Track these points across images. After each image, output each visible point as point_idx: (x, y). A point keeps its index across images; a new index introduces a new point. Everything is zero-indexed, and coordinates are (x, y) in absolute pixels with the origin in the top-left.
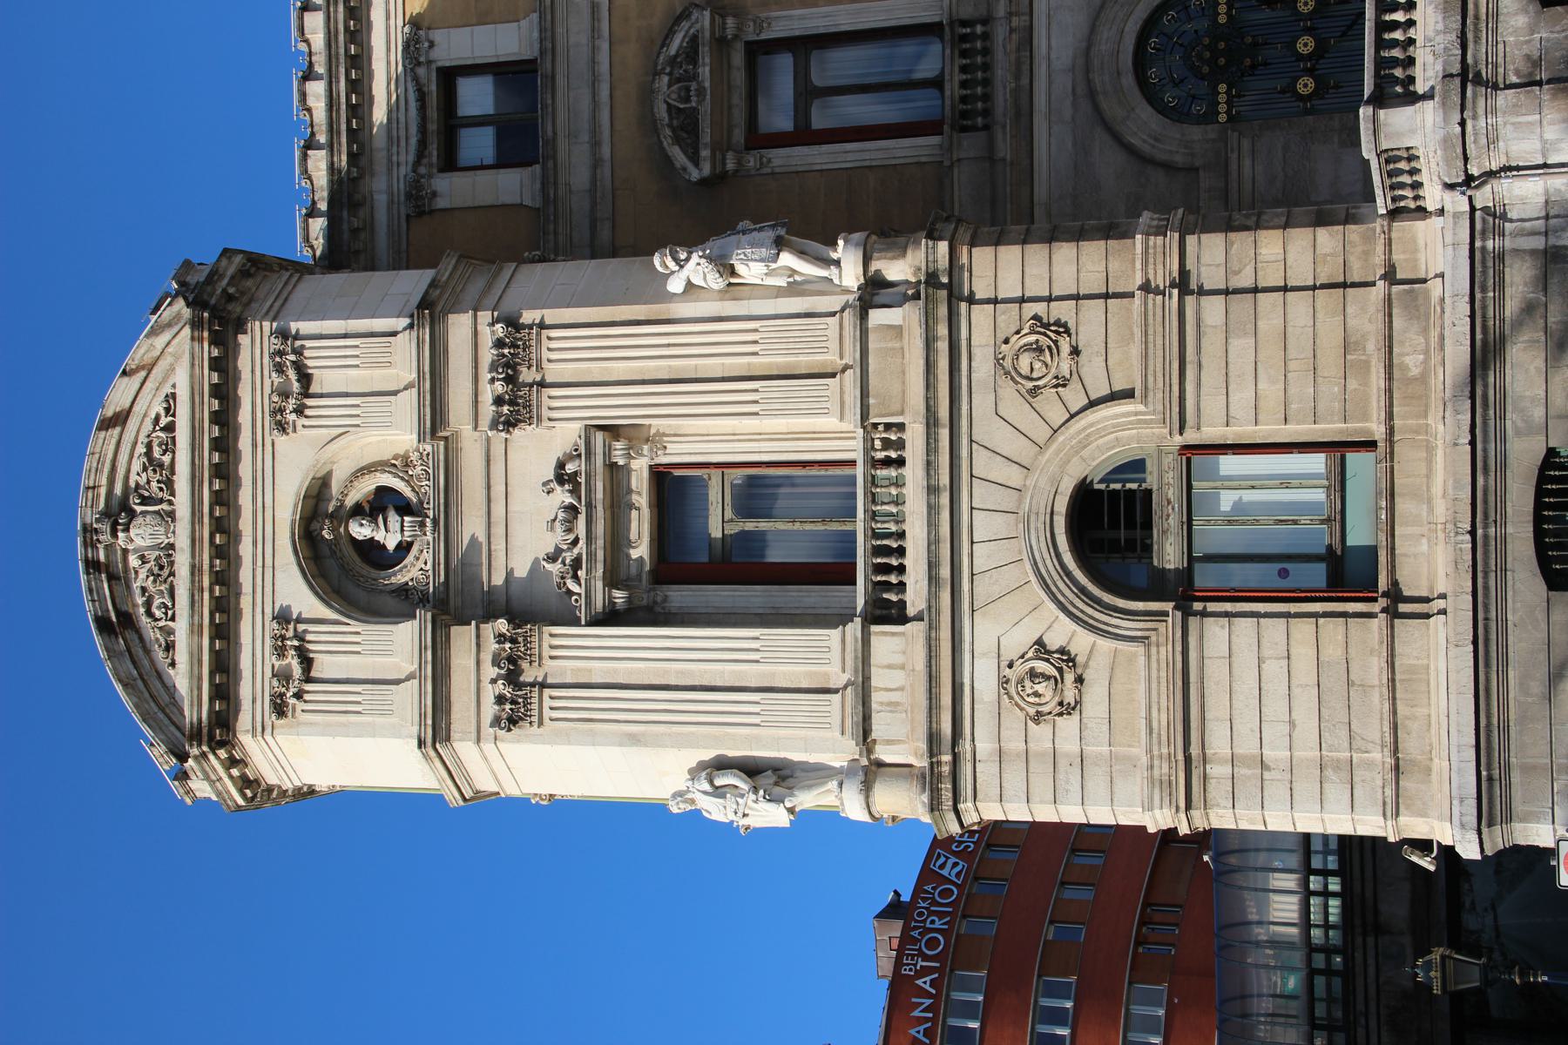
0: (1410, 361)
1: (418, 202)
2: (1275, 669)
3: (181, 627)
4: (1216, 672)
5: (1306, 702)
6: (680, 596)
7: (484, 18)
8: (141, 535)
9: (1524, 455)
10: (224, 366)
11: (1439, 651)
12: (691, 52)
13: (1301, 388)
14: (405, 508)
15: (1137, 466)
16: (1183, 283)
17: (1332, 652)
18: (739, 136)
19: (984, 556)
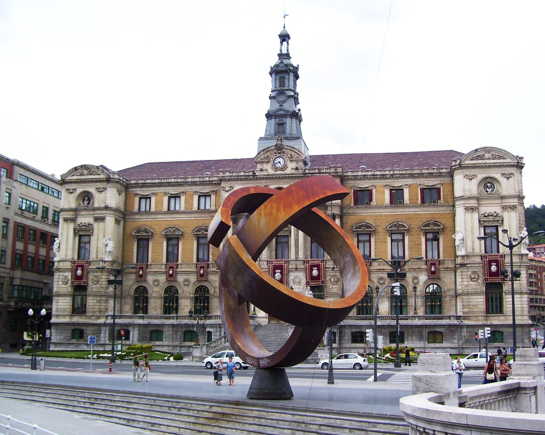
0: (92, 318)
2: (66, 304)
4: (66, 298)
6: (77, 238)
7: (156, 203)
8: (85, 172)
9: (84, 328)
10: (103, 181)
11: (67, 320)
13: (91, 307)
14: (88, 204)
15: (86, 290)
16: (101, 296)
17: (67, 310)
18: (139, 237)
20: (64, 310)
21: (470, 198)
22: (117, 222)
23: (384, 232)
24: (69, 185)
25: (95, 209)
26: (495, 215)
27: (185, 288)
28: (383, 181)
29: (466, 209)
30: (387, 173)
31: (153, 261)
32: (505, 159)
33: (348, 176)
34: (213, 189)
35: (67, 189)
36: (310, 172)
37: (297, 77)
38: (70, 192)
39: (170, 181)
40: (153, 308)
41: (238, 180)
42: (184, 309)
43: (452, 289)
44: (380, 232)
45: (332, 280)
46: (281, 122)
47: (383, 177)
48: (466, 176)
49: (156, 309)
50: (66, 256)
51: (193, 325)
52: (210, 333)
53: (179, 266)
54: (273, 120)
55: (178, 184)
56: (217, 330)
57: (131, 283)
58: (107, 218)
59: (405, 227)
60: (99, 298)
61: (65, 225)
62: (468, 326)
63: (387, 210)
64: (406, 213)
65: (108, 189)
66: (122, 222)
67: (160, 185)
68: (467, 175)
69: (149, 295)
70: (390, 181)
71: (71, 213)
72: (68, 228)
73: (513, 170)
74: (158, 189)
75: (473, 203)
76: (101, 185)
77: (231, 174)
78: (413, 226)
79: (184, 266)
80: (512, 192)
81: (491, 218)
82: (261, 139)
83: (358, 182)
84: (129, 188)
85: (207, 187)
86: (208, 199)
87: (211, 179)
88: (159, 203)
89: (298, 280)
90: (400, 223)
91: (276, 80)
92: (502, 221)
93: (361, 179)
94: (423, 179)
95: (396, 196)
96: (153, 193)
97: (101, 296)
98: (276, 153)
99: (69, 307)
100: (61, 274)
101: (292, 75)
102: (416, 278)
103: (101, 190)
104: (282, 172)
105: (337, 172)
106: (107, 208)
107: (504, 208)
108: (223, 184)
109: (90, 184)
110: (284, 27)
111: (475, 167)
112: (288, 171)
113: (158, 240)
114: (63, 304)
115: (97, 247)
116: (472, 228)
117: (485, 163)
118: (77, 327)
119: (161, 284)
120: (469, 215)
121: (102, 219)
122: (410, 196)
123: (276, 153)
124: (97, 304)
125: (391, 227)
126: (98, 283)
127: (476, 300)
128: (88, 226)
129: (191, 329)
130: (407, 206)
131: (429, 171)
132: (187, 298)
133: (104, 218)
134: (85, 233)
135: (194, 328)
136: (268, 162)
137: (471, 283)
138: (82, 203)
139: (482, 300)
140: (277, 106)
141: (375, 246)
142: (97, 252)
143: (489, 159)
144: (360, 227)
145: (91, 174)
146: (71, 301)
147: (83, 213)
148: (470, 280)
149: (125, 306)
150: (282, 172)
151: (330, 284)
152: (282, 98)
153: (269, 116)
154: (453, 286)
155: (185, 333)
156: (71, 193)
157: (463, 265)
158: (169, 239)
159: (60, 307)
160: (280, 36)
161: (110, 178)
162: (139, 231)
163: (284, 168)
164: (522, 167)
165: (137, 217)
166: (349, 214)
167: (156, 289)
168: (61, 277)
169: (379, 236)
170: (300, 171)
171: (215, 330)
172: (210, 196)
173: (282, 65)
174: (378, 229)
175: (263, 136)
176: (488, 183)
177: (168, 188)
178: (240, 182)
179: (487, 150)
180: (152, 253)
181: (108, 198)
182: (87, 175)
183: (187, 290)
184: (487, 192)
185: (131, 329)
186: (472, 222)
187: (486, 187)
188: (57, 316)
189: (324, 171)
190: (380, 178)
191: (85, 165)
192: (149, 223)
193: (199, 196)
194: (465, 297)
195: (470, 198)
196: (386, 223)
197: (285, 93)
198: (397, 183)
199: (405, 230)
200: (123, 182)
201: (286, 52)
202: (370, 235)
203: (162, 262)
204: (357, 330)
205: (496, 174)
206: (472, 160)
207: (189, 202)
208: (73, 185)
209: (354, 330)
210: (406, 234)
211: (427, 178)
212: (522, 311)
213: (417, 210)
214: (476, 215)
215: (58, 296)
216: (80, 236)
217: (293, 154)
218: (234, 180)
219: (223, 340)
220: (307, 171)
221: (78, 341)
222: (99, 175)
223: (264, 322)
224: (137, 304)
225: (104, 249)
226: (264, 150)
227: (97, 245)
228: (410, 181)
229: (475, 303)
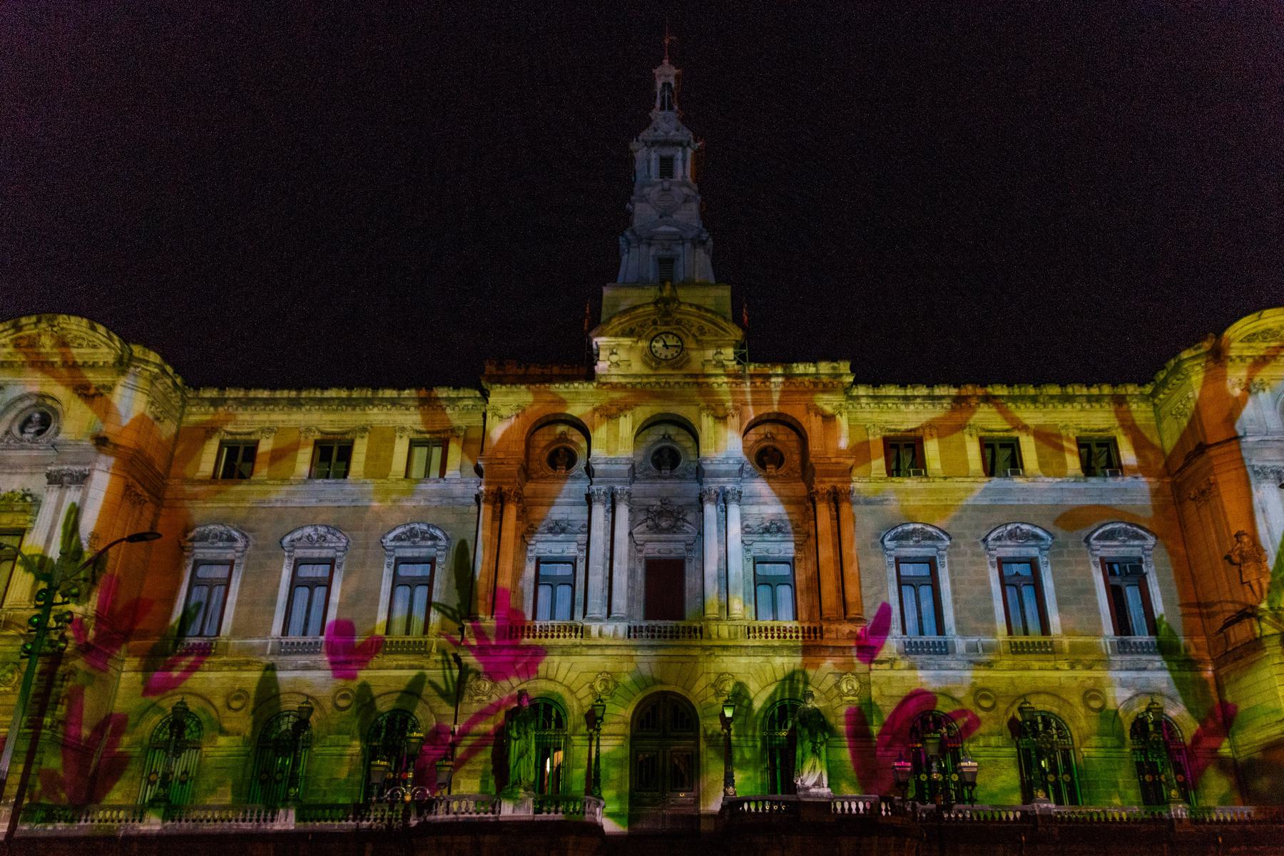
45: (844, 688)
59: (1042, 539)
74: (285, 417)
90: (1025, 527)
123: (655, 323)
138: (16, 431)
193: (413, 444)
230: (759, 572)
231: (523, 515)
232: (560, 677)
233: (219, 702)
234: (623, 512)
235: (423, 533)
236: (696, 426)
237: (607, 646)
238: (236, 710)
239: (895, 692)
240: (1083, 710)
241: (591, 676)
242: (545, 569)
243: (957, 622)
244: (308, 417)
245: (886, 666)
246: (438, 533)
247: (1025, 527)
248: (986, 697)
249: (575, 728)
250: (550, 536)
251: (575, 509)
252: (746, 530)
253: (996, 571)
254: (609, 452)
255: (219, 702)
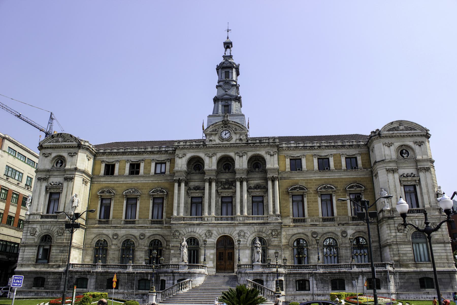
0: (54, 267)
1: (102, 162)
3: (52, 144)
5: (28, 256)
6: (48, 195)
7: (119, 169)
8: (60, 139)
12: (110, 193)
14: (61, 166)
18: (103, 197)
19: (45, 226)
20: (29, 259)
21: (390, 162)
22: (85, 182)
23: (314, 193)
24: (46, 150)
25: (65, 171)
26: (413, 175)
27: (140, 241)
28: (312, 151)
29: (387, 171)
30: (315, 145)
31: (113, 218)
32: (416, 130)
33: (282, 147)
34: (168, 158)
35: (44, 154)
36: (252, 142)
37: (238, 74)
38: (46, 156)
39: (132, 150)
40: (112, 259)
41: (190, 148)
42: (139, 260)
43: (375, 242)
44: (312, 193)
45: (273, 233)
46: (227, 104)
47: (312, 148)
48: (385, 144)
49: (114, 260)
50: (37, 210)
51: (147, 274)
52: (163, 282)
53: (137, 222)
54: (220, 102)
55: (138, 153)
56: (170, 278)
57: (93, 236)
58: (76, 178)
59: (333, 188)
60: (62, 249)
61: (39, 184)
62: (400, 273)
63: (316, 175)
64: (333, 177)
65: (79, 154)
66: (89, 184)
67: (124, 153)
68: (385, 143)
69: (108, 248)
70: (317, 151)
71: (45, 173)
72: (41, 186)
73: (423, 139)
74: (121, 157)
75: (392, 166)
76: (72, 150)
77: (184, 144)
78: (339, 188)
79: (140, 222)
80: (425, 157)
81: (410, 178)
82: (210, 116)
83: (291, 152)
84: (96, 157)
85: (163, 156)
86: (163, 166)
87: (167, 149)
88: (122, 169)
89: (242, 234)
90: (328, 185)
91: (222, 73)
92: (419, 180)
93: (293, 150)
94: (345, 150)
95: (324, 164)
96: (118, 161)
97: (65, 246)
98: (222, 127)
99: (34, 256)
100: (30, 226)
101: (234, 70)
102: (344, 232)
103: (73, 155)
104: (228, 142)
105: (275, 142)
106: (76, 169)
107: (418, 170)
108: (177, 152)
109: (64, 149)
110: (228, 38)
111: (391, 137)
112: (233, 141)
113: (119, 200)
114: (28, 254)
115: (65, 203)
116: (395, 186)
117: (400, 133)
118: (39, 276)
119: (119, 238)
120: (390, 175)
121: (72, 179)
122: (335, 163)
123: (222, 127)
124: (60, 254)
125: (321, 189)
126: (62, 234)
127: (405, 249)
128: (59, 185)
129: (145, 278)
130: (333, 171)
131: (348, 144)
132: (142, 251)
133: (73, 178)
134: (55, 191)
135: (148, 276)
136: (216, 134)
137: (398, 234)
138: (55, 165)
139: (410, 249)
140: (222, 92)
141: (308, 205)
142: (64, 207)
143: (402, 130)
144: (295, 189)
145: (65, 142)
146: (36, 251)
147: (56, 173)
148: (397, 231)
149: (87, 257)
150: (228, 142)
151: (271, 237)
152: (226, 87)
153: (216, 100)
154: (377, 239)
155: (139, 281)
156: (47, 157)
157: (389, 218)
158: (128, 199)
159: (25, 256)
160: (225, 43)
161: (81, 145)
162: (103, 192)
163: (230, 138)
164: (429, 137)
165: (102, 180)
166: (285, 178)
167: (115, 242)
168: (29, 229)
169: (311, 196)
170: (244, 142)
171: (168, 279)
172: (165, 163)
173: (226, 63)
174: (309, 191)
175: (211, 114)
176: (404, 151)
177: (130, 156)
178: (191, 150)
179: (401, 123)
180: (114, 210)
181: (78, 161)
182: (62, 142)
183: (143, 244)
184: (403, 157)
185: (88, 277)
186: (394, 181)
187: (401, 153)
188: (22, 265)
189: (264, 141)
190: (309, 149)
191: (61, 134)
192: (112, 185)
193: (156, 164)
194: (394, 247)
195: (390, 162)
196: (316, 185)
197: (230, 84)
198: (324, 153)
199: (333, 191)
200: (93, 150)
201: (229, 55)
202: (302, 196)
203: (122, 218)
204: (301, 278)
205: (409, 142)
206: (389, 131)
207: (147, 169)
208: (49, 150)
209: (298, 278)
210: (333, 194)
211: (348, 149)
212: (448, 259)
213: (341, 174)
214: (397, 176)
215: (25, 246)
216: (51, 194)
217: (237, 128)
218: (187, 148)
219: (175, 288)
220: (250, 142)
221: (38, 289)
222: (72, 142)
223: (212, 272)
224: (97, 256)
225: (71, 204)
226: (213, 125)
227: (65, 201)
228: (334, 151)
229: (404, 252)
230: (254, 200)
231: (186, 185)
232: (197, 232)
233: (111, 237)
234: (214, 185)
235: (160, 190)
236: (234, 159)
237: (209, 223)
238: (115, 239)
239: (290, 233)
240: (341, 237)
241: (205, 231)
242: (194, 201)
243: (308, 213)
244: (128, 157)
245: (288, 226)
246: (164, 190)
247: (328, 185)
248: (315, 234)
249: (201, 245)
250: (195, 191)
251: (201, 183)
252: (249, 188)
253: (320, 198)
254: (209, 167)
255: (111, 237)
